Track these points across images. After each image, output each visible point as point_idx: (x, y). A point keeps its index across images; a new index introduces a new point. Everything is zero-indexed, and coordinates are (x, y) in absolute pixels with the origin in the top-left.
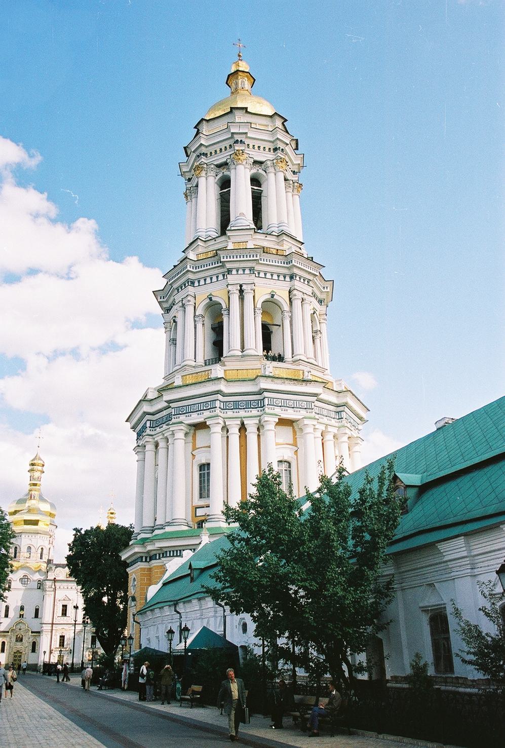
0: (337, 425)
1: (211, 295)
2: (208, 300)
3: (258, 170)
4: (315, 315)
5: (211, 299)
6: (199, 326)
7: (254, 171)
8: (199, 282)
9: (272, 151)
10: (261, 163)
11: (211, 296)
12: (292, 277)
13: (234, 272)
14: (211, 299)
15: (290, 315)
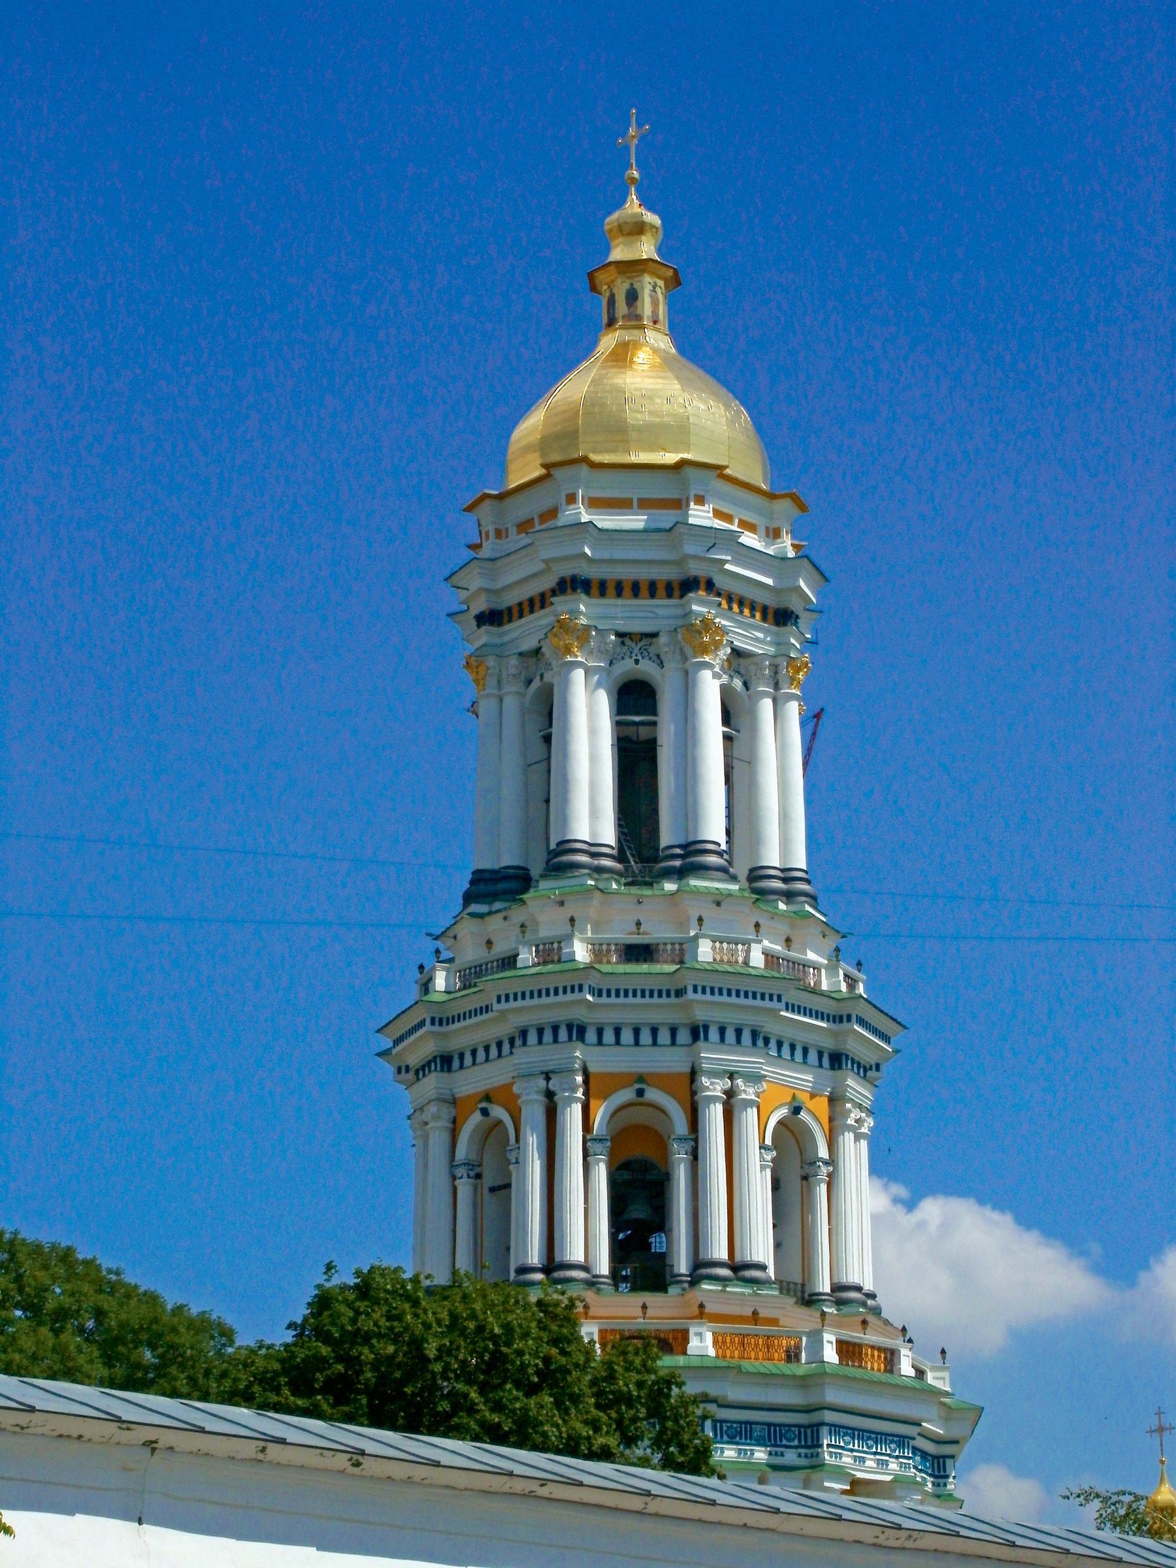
0: (803, 1462)
1: (487, 1098)
2: (477, 1117)
3: (637, 662)
4: (803, 1115)
5: (485, 1112)
6: (464, 1188)
7: (626, 667)
8: (462, 1056)
9: (677, 593)
10: (654, 635)
11: (483, 1105)
12: (697, 1032)
13: (532, 1038)
14: (485, 1112)
15: (693, 1143)
